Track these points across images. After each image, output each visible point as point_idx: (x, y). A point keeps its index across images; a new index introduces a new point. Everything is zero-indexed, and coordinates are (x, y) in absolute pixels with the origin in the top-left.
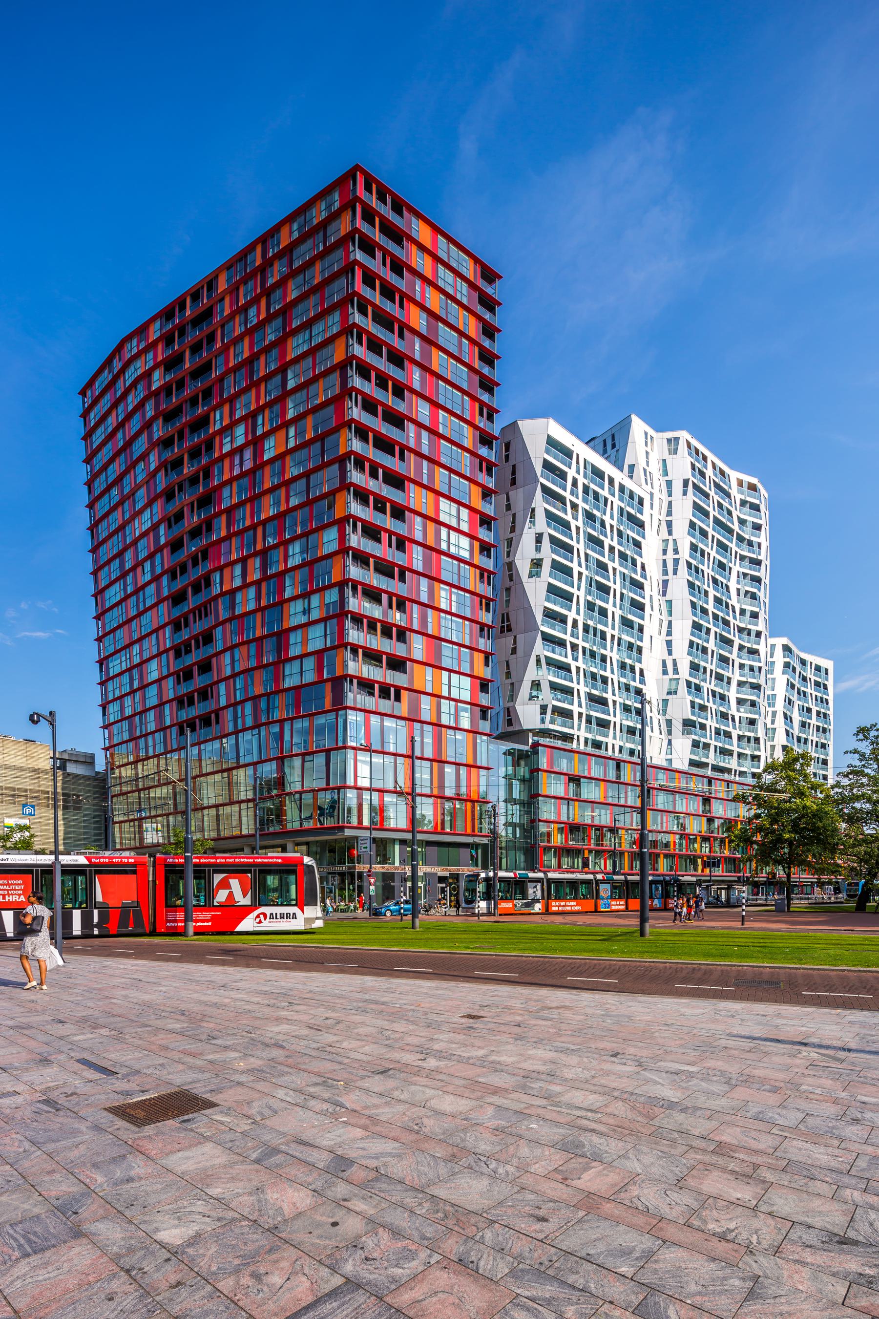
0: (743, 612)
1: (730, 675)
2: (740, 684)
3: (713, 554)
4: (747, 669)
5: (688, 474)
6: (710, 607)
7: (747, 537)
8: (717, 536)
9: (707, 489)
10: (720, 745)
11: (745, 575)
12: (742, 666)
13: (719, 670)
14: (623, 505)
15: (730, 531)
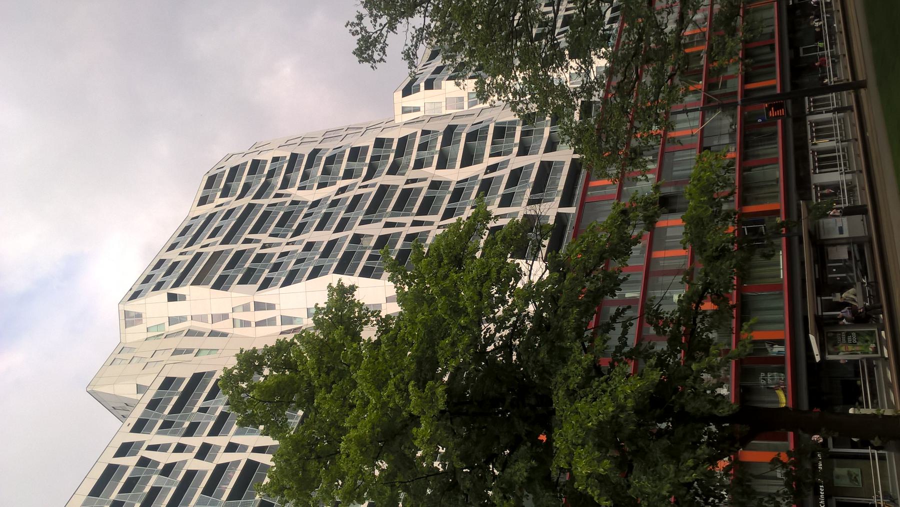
0: (348, 174)
1: (425, 185)
2: (442, 165)
3: (264, 238)
4: (425, 154)
5: (162, 295)
6: (325, 236)
7: (263, 180)
8: (246, 235)
9: (189, 258)
10: (528, 191)
11: (305, 177)
12: (419, 164)
13: (415, 210)
14: (160, 422)
15: (251, 207)
